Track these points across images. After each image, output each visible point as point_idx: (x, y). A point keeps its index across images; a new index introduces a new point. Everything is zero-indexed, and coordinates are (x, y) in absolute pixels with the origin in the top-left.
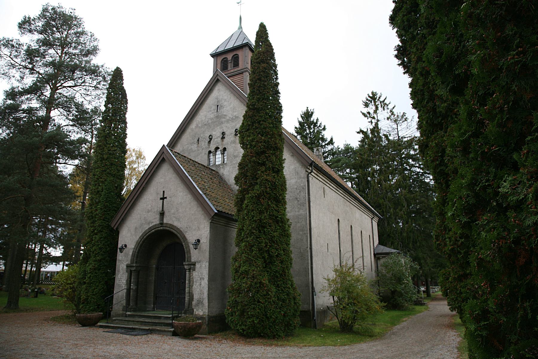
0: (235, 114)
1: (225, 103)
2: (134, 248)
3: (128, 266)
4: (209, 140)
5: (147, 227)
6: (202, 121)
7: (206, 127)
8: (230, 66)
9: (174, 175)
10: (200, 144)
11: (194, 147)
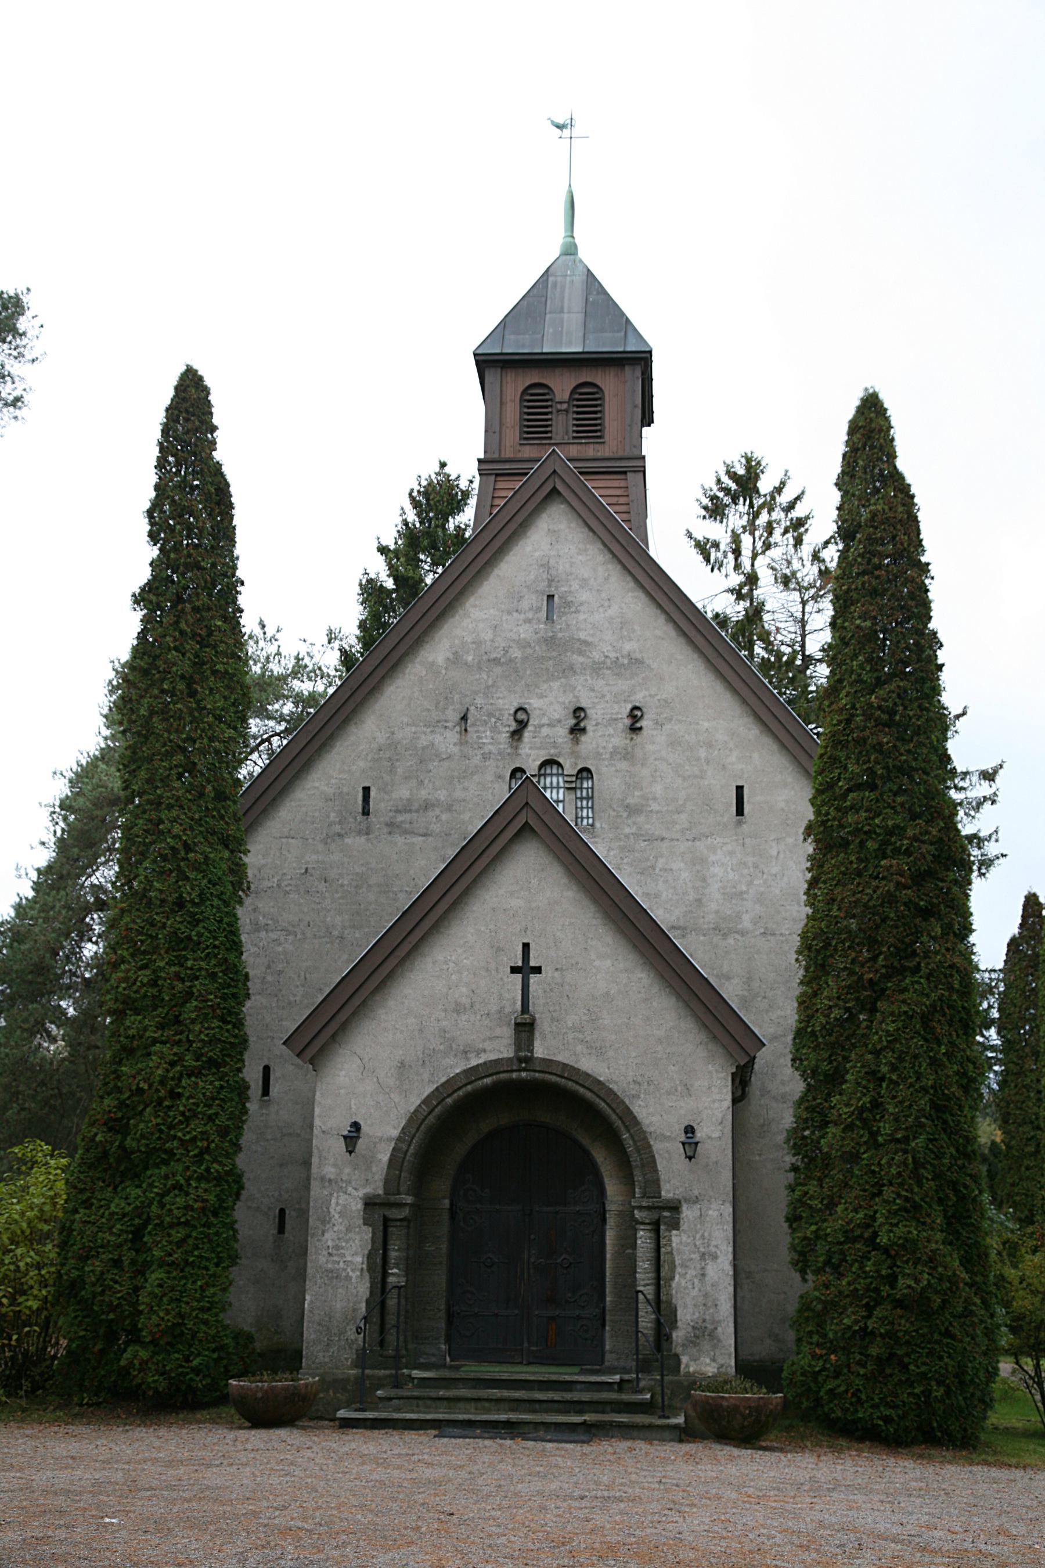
0: (628, 647)
1: (584, 596)
2: (399, 1139)
3: (370, 1203)
4: (514, 726)
5: (458, 1067)
6: (478, 643)
7: (498, 670)
8: (562, 425)
9: (570, 894)
10: (472, 735)
11: (447, 741)
